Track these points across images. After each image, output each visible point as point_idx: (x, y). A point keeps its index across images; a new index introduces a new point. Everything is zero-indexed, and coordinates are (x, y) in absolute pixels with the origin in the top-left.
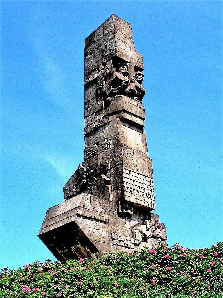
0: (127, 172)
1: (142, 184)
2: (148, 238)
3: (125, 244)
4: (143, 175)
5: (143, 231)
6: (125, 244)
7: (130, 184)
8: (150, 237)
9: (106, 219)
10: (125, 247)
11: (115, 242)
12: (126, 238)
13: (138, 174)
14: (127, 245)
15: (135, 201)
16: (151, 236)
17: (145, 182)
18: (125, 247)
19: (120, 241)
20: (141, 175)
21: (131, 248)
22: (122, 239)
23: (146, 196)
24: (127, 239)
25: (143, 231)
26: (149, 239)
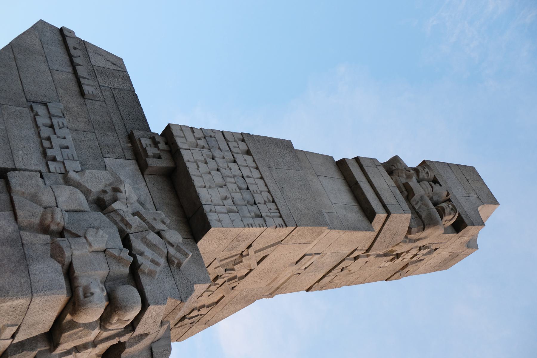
0: (243, 146)
1: (248, 189)
2: (109, 217)
3: (49, 139)
4: (269, 192)
6: (49, 139)
7: (219, 148)
8: (118, 219)
9: (91, 93)
11: (40, 110)
13: (262, 178)
14: (52, 147)
15: (186, 155)
16: (122, 225)
17: (259, 199)
20: (266, 185)
23: (226, 198)
24: (67, 148)
26: (107, 219)
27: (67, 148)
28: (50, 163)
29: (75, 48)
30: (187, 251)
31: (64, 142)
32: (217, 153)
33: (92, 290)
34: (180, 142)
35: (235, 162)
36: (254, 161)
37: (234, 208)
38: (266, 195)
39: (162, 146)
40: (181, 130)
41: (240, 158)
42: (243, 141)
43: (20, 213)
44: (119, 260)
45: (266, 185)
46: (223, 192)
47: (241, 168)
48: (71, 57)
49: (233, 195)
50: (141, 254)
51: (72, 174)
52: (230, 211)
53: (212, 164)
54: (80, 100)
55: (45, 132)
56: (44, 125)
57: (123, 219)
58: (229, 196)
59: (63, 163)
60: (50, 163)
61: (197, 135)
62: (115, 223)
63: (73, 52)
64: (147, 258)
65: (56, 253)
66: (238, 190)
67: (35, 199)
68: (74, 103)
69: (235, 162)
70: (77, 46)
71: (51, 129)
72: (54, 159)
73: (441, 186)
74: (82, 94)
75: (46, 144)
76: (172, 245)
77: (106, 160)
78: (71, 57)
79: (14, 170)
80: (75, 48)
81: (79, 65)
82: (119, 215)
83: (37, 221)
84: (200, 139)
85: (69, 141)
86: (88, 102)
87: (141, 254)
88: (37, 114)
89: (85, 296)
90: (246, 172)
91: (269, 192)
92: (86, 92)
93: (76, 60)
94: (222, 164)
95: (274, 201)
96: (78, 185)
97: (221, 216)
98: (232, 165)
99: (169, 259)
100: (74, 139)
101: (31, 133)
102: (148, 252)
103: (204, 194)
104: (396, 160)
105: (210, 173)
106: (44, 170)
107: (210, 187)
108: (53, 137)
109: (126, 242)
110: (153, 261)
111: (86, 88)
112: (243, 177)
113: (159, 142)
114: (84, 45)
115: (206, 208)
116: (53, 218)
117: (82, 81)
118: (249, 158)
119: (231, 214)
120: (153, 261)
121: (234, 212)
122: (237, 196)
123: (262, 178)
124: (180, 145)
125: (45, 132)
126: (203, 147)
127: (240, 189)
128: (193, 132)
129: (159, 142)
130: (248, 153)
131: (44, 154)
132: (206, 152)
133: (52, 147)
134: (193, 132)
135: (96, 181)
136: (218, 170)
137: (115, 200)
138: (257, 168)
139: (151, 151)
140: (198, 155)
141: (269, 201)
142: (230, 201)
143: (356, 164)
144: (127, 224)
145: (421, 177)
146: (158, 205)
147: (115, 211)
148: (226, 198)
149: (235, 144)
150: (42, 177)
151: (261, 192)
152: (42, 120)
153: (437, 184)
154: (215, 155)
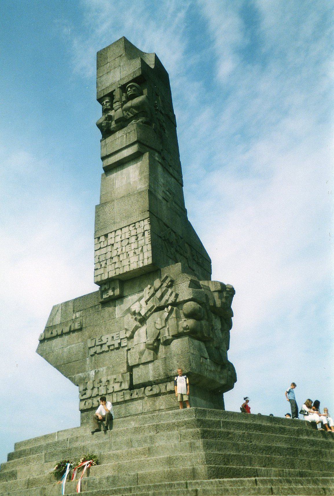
0: (102, 239)
1: (128, 239)
3: (109, 347)
4: (129, 226)
5: (135, 311)
6: (109, 347)
8: (149, 313)
10: (111, 350)
12: (109, 336)
13: (121, 229)
14: (114, 345)
15: (112, 274)
16: (153, 310)
17: (133, 233)
18: (111, 350)
19: (101, 345)
20: (125, 227)
21: (123, 347)
22: (104, 341)
23: (135, 253)
25: (135, 311)
27: (113, 337)
28: (122, 346)
29: (52, 333)
30: (165, 276)
31: (110, 339)
32: (109, 256)
33: (185, 326)
34: (105, 277)
35: (113, 245)
36: (111, 232)
37: (140, 249)
38: (131, 228)
39: (106, 287)
40: (97, 276)
41: (110, 241)
42: (99, 238)
43: (149, 360)
44: (170, 313)
45: (125, 227)
46: (131, 254)
47: (116, 241)
48: (57, 336)
49: (133, 248)
50: (167, 301)
51: (128, 335)
52: (142, 251)
53: (115, 259)
54: (84, 330)
55: (105, 348)
56: (101, 349)
57: (150, 310)
58: (133, 251)
59: (121, 339)
60: (122, 346)
61: (99, 267)
62: (151, 314)
63: (55, 334)
64: (169, 298)
65: (167, 343)
66: (130, 245)
67: (142, 353)
68: (86, 333)
69: (113, 245)
70: (50, 332)
71: (103, 346)
72: (120, 344)
73: (115, 90)
74: (80, 329)
75: (112, 348)
76: (162, 285)
77: (117, 317)
78: (57, 336)
79: (127, 362)
80: (52, 333)
81: (62, 331)
82: (147, 312)
83: (152, 352)
84: (101, 265)
85: (109, 336)
86: (84, 326)
87: (167, 301)
88: (95, 353)
89: (188, 329)
90: (118, 239)
91: (129, 226)
92: (79, 327)
93: (59, 332)
94: (115, 253)
95: (135, 223)
96: (133, 332)
97: (146, 257)
98: (115, 247)
99: (169, 287)
100: (108, 333)
101: (107, 355)
102: (166, 297)
103: (134, 266)
104: (99, 126)
105: (121, 261)
106: (126, 348)
107: (129, 262)
108: (108, 344)
109: (160, 309)
110: (171, 295)
111: (77, 326)
112: (122, 241)
113: (105, 288)
114: (48, 328)
115: (141, 265)
116: (151, 345)
117: (72, 329)
118: (110, 236)
119: (144, 251)
120: (171, 295)
121: (142, 248)
122: (134, 246)
123: (121, 229)
124: (106, 277)
125: (105, 348)
126: (106, 264)
127: (128, 244)
128: (97, 269)
129: (105, 288)
130: (106, 236)
131: (117, 349)
132: (108, 262)
133: (114, 345)
134: (97, 269)
135: (131, 322)
136: (119, 256)
137: (139, 314)
138: (115, 231)
139: (111, 293)
140: (110, 268)
141: (135, 226)
142: (136, 251)
143: (106, 160)
144: (152, 308)
145: (109, 107)
146: (140, 289)
147: (145, 314)
148: (135, 253)
149: (102, 243)
150: (129, 350)
151: (130, 230)
152: (98, 349)
153: (114, 94)
154: (110, 257)
